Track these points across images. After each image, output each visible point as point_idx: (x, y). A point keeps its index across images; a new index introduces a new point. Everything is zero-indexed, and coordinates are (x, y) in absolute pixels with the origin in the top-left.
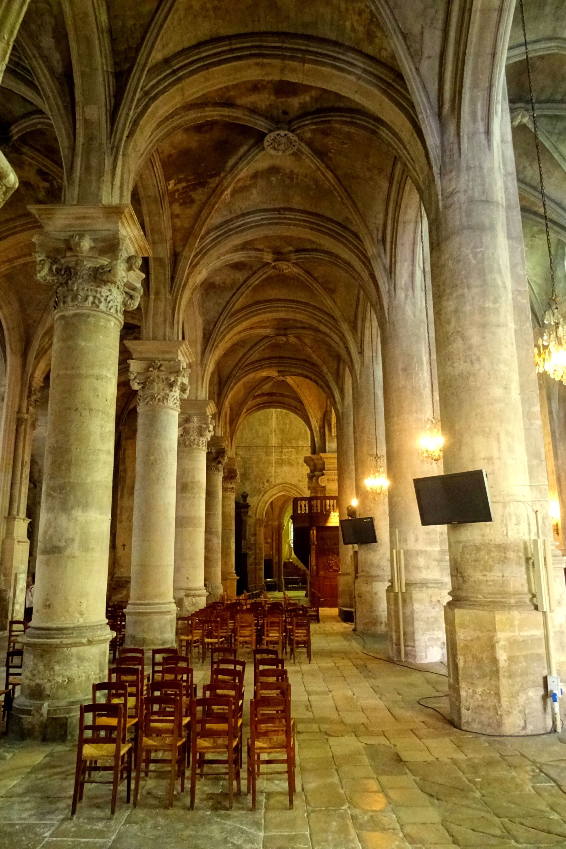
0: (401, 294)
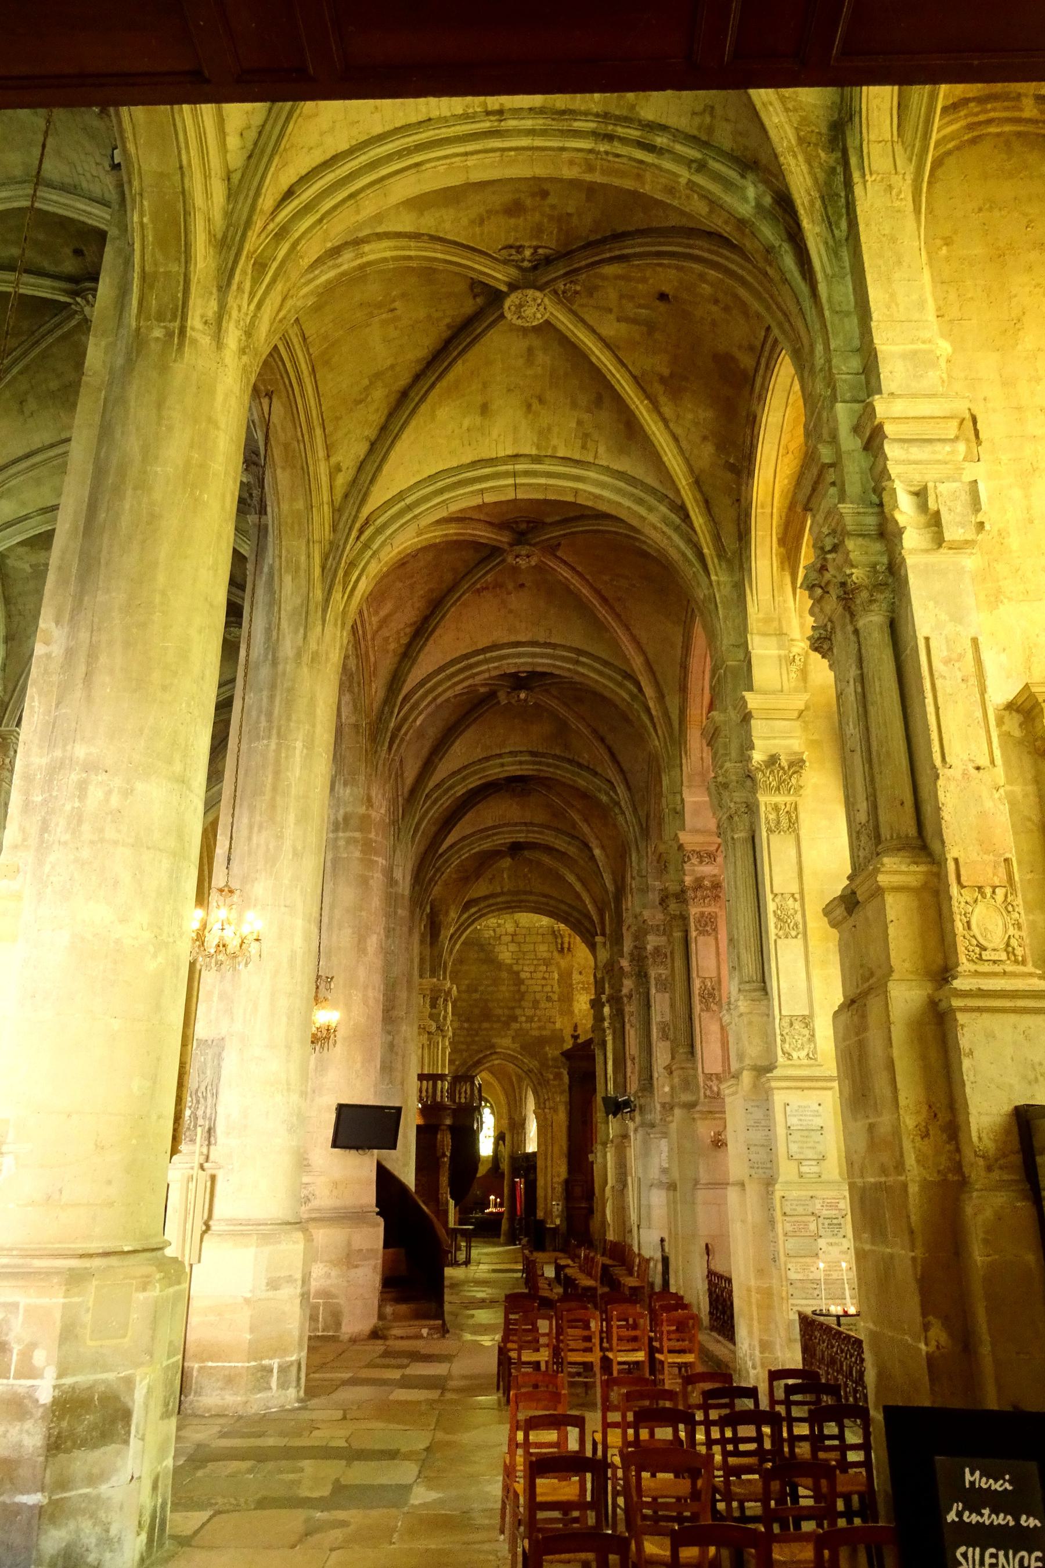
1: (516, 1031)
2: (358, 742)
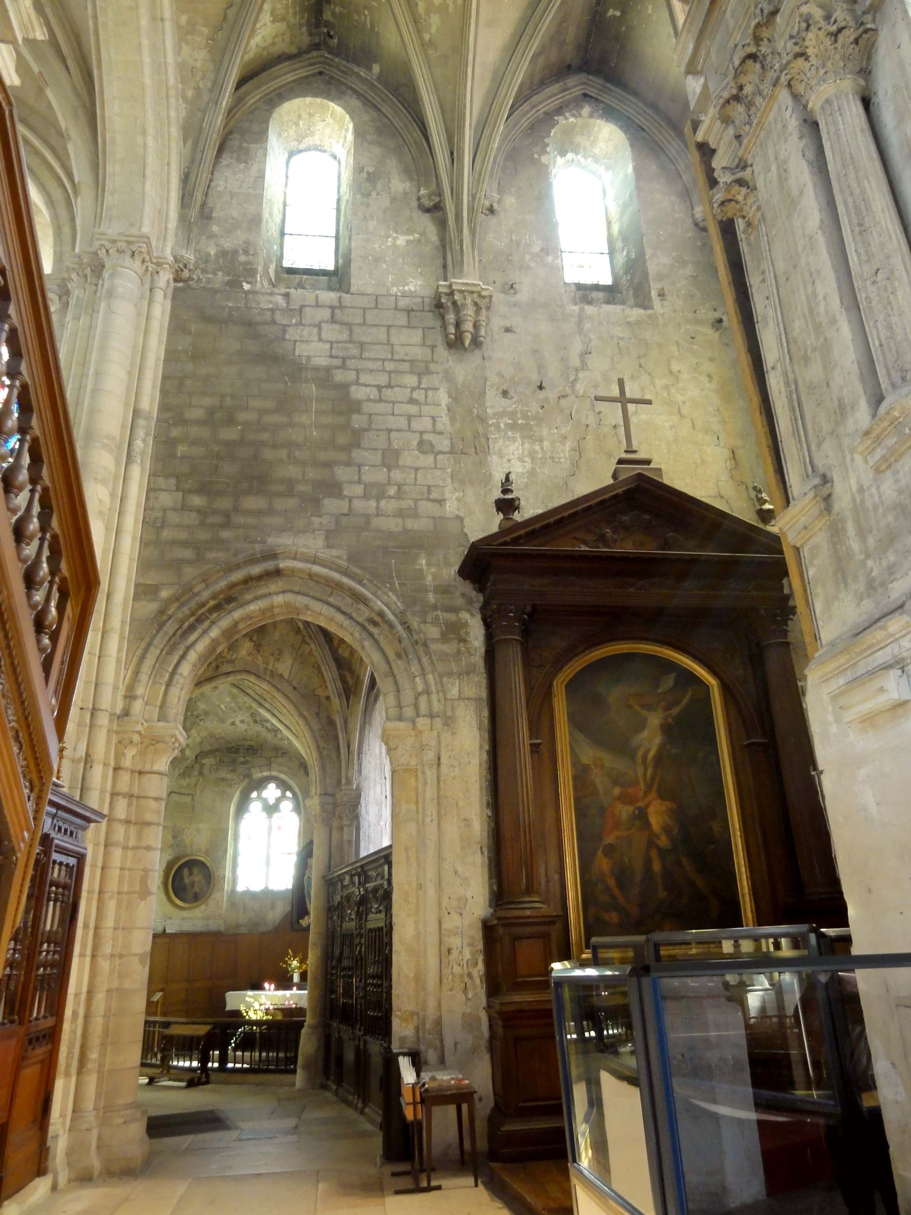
1: (339, 517)
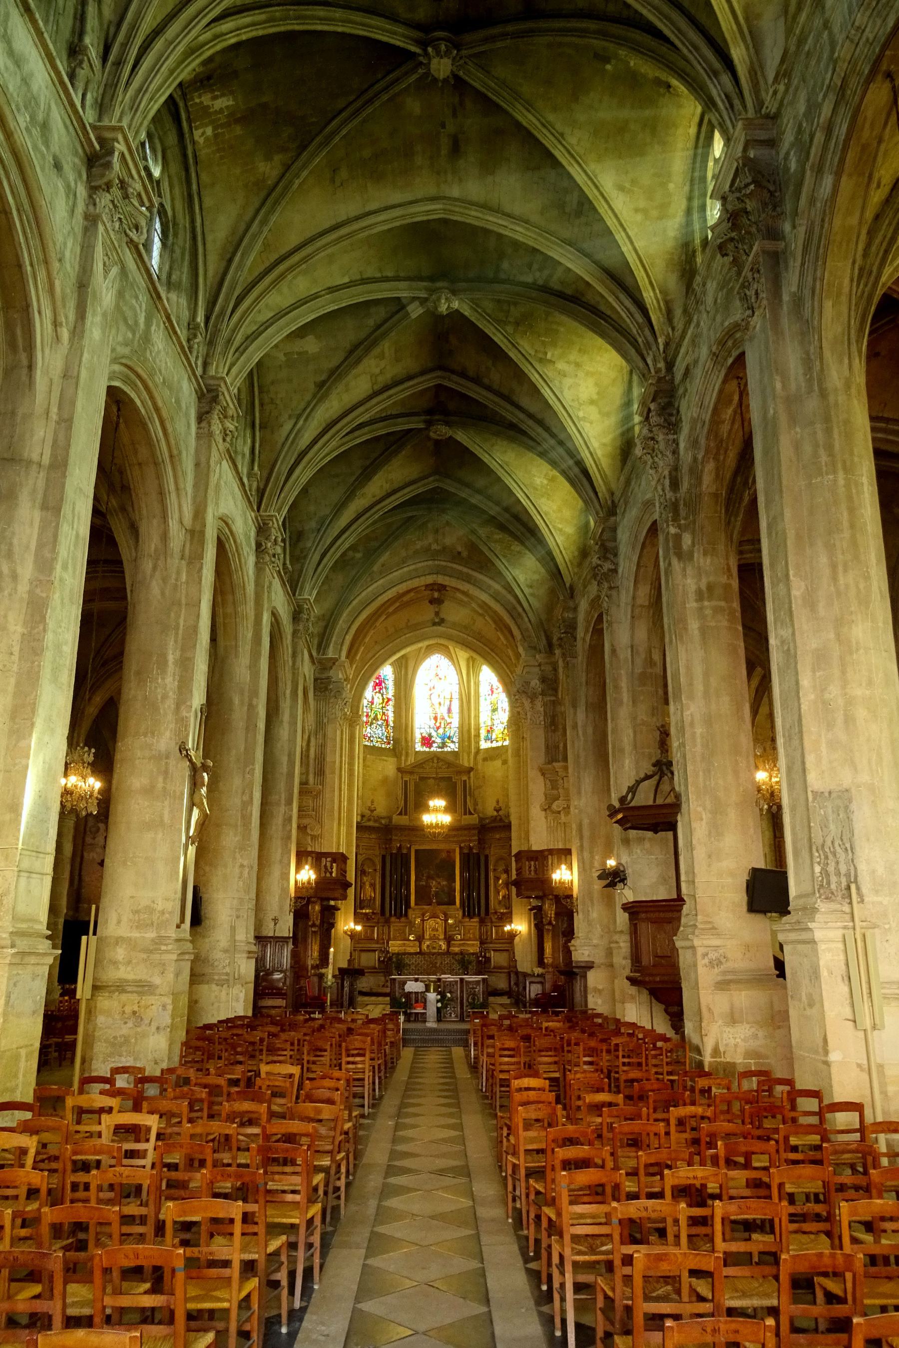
0: (147, 565)
2: (716, 512)
